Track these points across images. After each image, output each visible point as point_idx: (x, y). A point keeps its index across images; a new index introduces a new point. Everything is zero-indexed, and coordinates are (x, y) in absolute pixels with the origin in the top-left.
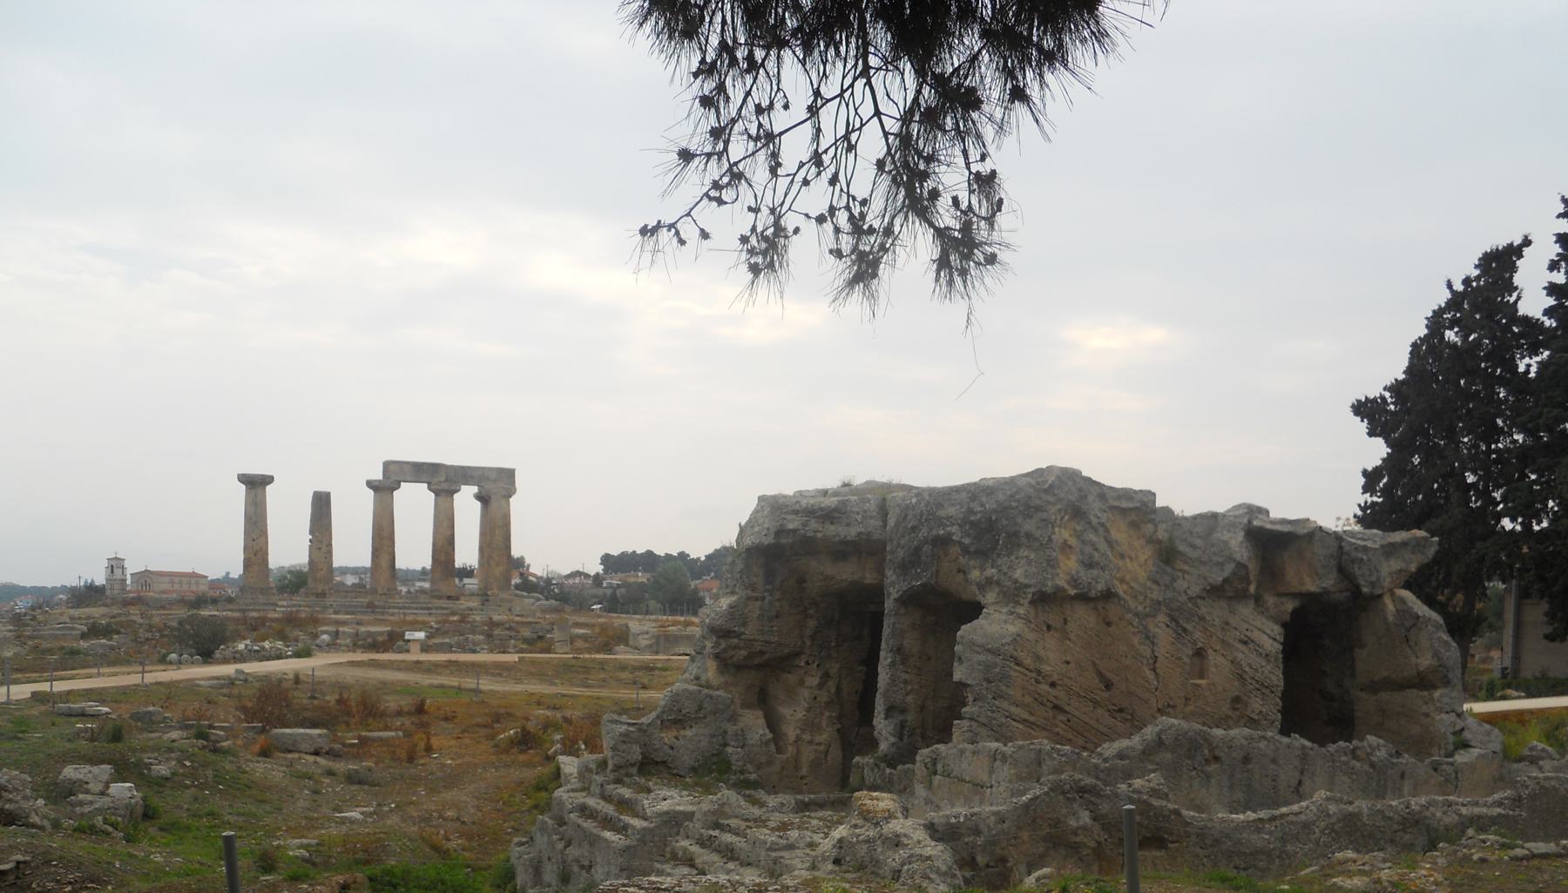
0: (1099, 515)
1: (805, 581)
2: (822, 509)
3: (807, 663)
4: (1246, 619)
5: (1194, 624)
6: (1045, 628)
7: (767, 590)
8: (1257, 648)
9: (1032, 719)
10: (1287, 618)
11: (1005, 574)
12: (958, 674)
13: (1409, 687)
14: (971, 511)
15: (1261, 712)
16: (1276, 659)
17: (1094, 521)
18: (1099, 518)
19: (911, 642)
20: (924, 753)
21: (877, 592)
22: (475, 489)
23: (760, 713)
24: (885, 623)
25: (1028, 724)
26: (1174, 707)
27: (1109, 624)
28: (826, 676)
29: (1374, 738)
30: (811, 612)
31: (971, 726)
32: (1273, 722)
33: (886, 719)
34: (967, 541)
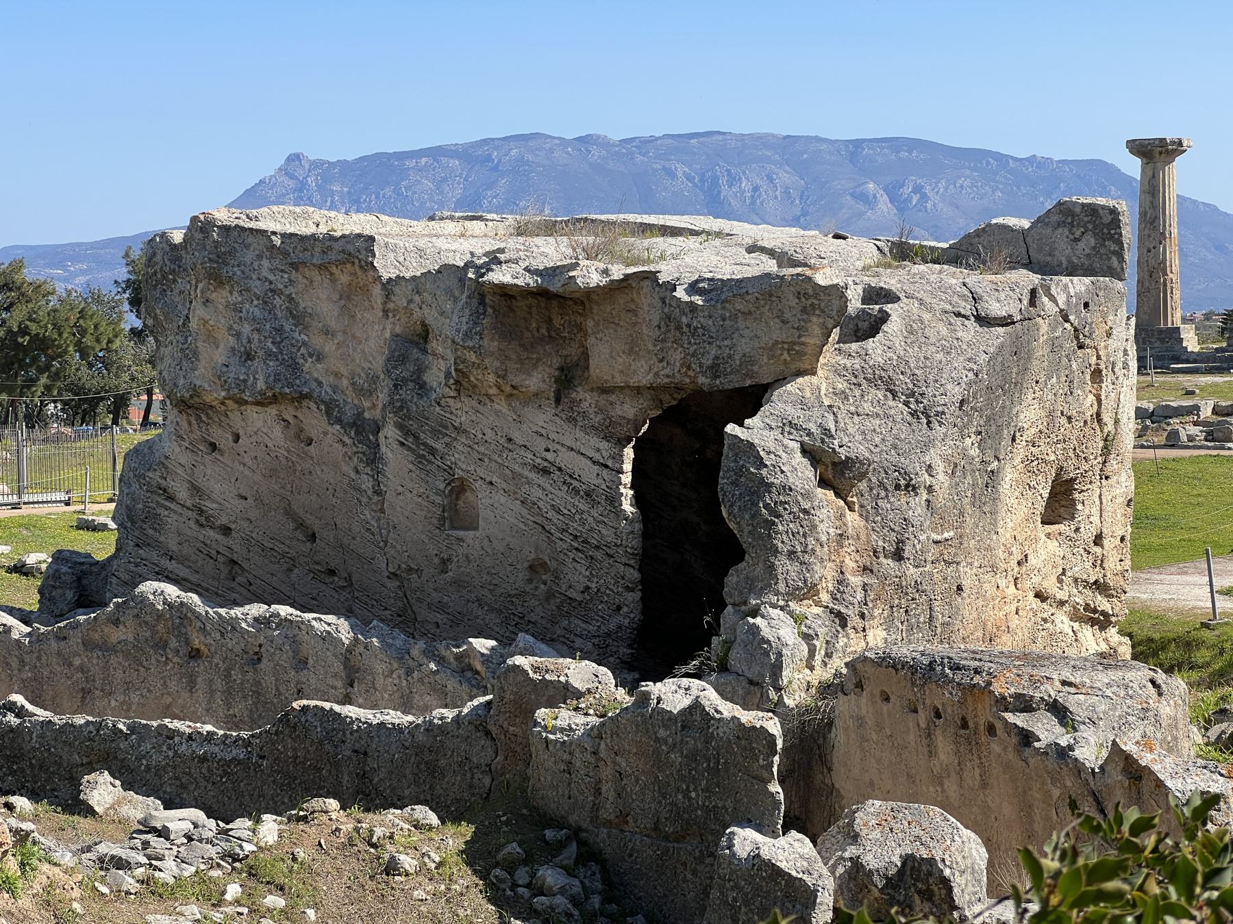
0: (272, 278)
4: (543, 432)
5: (447, 439)
8: (569, 480)
15: (588, 588)
18: (271, 283)
26: (418, 571)
27: (310, 442)
32: (619, 608)
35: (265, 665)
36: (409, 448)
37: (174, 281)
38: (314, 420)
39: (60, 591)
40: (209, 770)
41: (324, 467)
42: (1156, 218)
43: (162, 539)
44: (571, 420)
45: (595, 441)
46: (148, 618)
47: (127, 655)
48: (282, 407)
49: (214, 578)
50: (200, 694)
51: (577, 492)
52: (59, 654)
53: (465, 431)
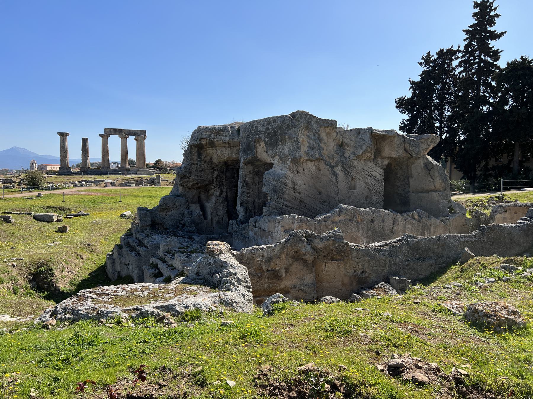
1: (212, 158)
3: (215, 187)
6: (296, 172)
7: (198, 161)
9: (292, 206)
10: (385, 167)
12: (264, 189)
13: (431, 191)
14: (268, 129)
16: (382, 182)
17: (314, 131)
19: (249, 179)
20: (251, 220)
21: (237, 161)
22: (134, 137)
23: (198, 205)
24: (240, 171)
25: (290, 208)
27: (320, 171)
28: (222, 192)
29: (420, 210)
31: (269, 209)
33: (241, 206)
34: (267, 140)
35: (376, 222)
36: (343, 171)
37: (292, 128)
38: (322, 165)
39: (146, 218)
40: (469, 244)
41: (324, 176)
42: (65, 147)
43: (284, 196)
44: (376, 165)
45: (380, 169)
46: (348, 213)
47: (343, 223)
48: (315, 162)
49: (297, 205)
50: (360, 232)
51: (376, 180)
52: (325, 225)
53: (355, 167)
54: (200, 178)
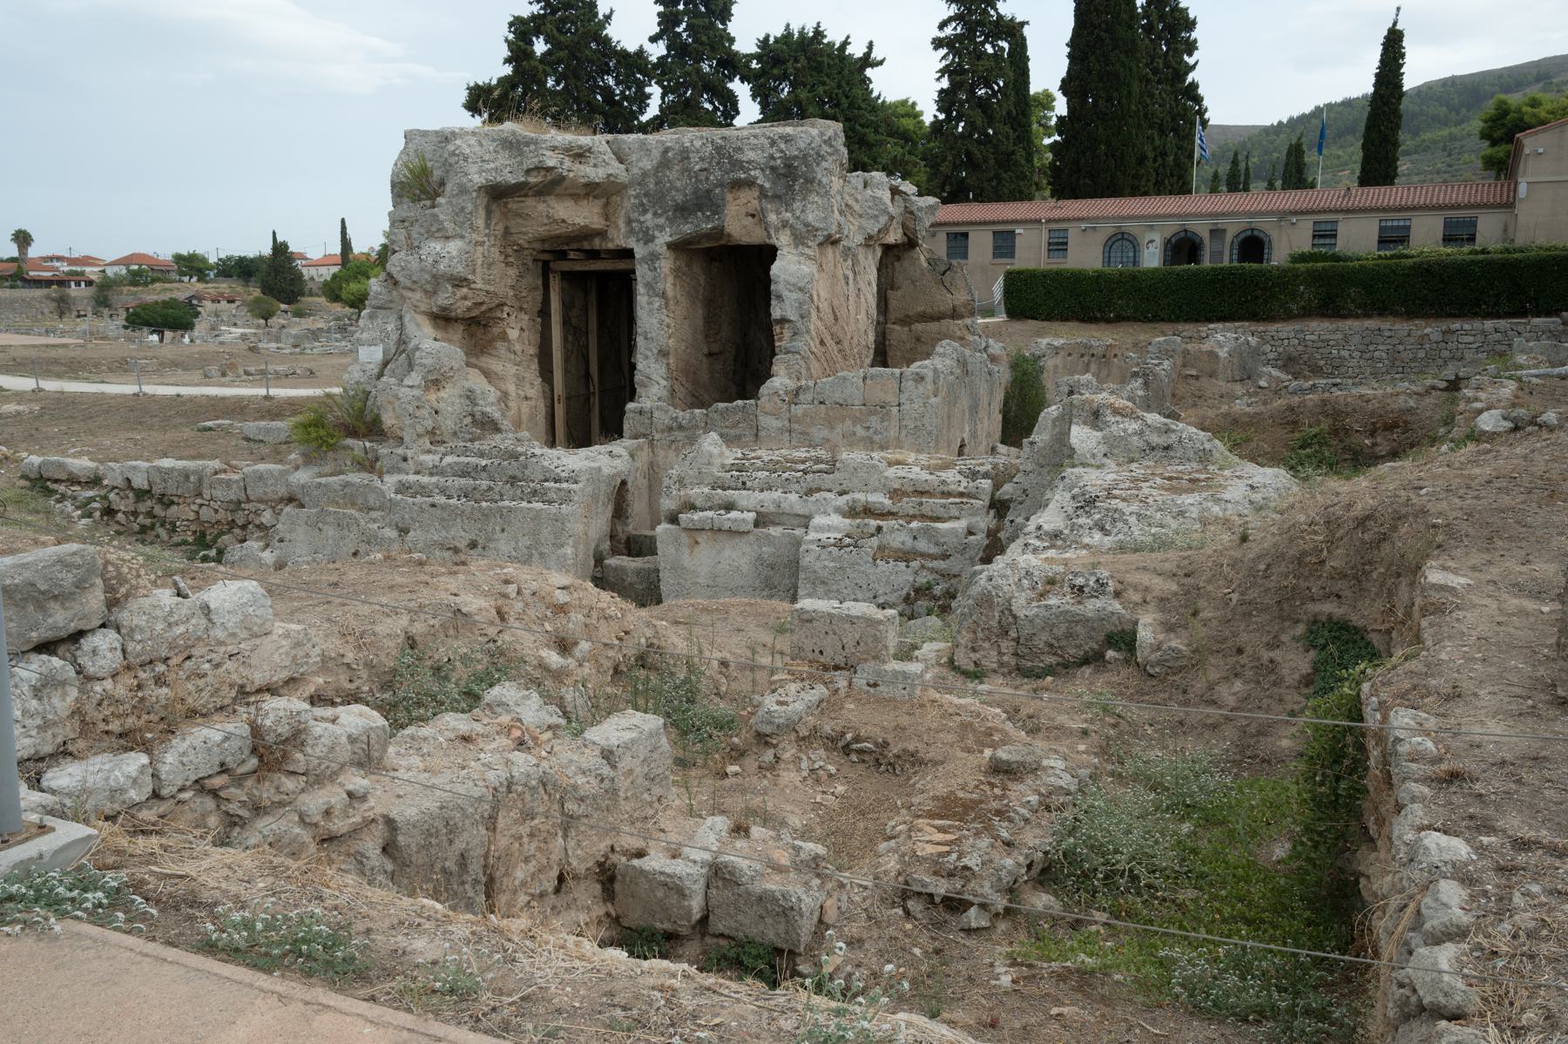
2: (580, 147)
11: (798, 218)
14: (772, 157)
30: (511, 259)
54: (488, 287)
